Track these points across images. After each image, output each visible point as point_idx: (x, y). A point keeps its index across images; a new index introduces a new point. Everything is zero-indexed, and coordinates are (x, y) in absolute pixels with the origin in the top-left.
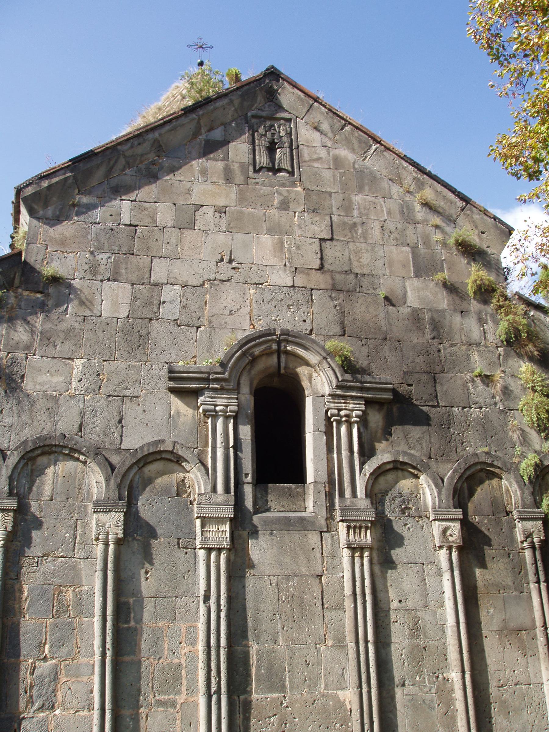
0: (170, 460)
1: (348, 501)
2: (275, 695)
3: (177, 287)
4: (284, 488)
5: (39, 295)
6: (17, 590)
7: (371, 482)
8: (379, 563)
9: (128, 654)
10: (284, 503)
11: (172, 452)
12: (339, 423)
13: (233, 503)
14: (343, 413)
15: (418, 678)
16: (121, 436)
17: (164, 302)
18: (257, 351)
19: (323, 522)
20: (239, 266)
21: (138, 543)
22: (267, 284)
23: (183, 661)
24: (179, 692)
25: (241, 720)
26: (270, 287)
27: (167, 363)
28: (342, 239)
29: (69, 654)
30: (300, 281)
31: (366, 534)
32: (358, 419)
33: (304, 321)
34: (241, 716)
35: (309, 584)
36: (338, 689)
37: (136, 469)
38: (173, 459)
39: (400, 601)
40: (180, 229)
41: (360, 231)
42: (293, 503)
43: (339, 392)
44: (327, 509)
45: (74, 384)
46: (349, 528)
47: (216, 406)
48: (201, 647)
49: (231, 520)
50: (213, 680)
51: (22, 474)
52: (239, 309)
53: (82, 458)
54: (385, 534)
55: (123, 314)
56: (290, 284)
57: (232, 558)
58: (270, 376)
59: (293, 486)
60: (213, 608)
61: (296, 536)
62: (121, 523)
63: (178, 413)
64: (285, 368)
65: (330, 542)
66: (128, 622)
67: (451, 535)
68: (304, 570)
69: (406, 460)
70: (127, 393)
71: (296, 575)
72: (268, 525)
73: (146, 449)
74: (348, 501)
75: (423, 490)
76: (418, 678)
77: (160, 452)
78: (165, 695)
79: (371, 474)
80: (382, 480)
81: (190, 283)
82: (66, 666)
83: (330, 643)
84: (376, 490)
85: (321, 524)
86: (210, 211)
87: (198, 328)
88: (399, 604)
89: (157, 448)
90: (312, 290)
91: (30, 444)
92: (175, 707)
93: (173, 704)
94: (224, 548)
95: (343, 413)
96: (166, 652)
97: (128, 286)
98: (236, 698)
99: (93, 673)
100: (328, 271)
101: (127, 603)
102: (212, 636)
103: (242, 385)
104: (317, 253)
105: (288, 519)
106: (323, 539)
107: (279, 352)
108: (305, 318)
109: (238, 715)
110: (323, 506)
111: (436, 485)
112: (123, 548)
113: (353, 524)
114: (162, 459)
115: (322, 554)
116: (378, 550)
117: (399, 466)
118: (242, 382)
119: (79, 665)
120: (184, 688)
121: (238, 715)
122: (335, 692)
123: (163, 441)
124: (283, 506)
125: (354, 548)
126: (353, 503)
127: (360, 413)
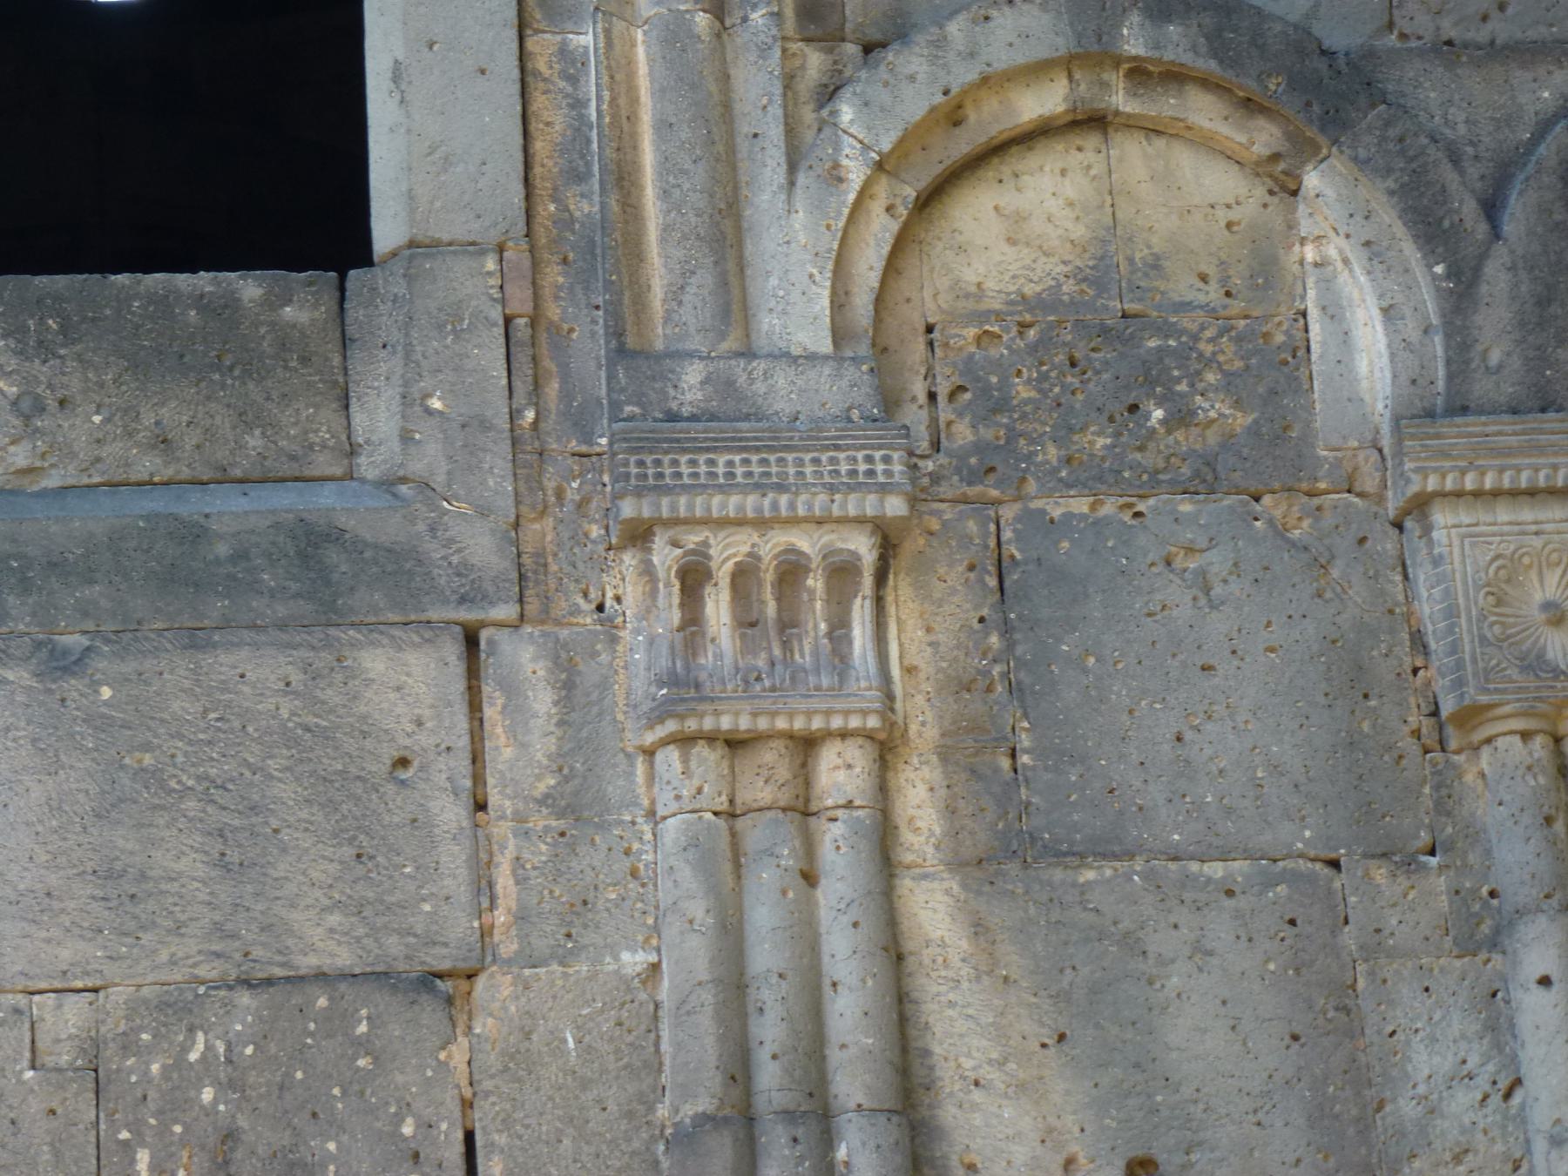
1: (692, 375)
4: (163, 304)
7: (880, 230)
8: (957, 864)
10: (172, 414)
19: (481, 547)
35: (363, 1045)
42: (247, 419)
44: (515, 442)
46: (693, 578)
54: (1007, 629)
59: (249, 287)
61: (259, 673)
65: (543, 701)
68: (324, 942)
71: (246, 983)
72: (25, 586)
74: (692, 375)
75: (1327, 284)
80: (977, 212)
85: (462, 571)
105: (194, 534)
106: (487, 689)
110: (485, 426)
111: (1431, 227)
113: (727, 551)
115: (481, 806)
116: (945, 755)
117: (1120, 100)
124: (163, 443)
125: (735, 744)
126: (724, 386)
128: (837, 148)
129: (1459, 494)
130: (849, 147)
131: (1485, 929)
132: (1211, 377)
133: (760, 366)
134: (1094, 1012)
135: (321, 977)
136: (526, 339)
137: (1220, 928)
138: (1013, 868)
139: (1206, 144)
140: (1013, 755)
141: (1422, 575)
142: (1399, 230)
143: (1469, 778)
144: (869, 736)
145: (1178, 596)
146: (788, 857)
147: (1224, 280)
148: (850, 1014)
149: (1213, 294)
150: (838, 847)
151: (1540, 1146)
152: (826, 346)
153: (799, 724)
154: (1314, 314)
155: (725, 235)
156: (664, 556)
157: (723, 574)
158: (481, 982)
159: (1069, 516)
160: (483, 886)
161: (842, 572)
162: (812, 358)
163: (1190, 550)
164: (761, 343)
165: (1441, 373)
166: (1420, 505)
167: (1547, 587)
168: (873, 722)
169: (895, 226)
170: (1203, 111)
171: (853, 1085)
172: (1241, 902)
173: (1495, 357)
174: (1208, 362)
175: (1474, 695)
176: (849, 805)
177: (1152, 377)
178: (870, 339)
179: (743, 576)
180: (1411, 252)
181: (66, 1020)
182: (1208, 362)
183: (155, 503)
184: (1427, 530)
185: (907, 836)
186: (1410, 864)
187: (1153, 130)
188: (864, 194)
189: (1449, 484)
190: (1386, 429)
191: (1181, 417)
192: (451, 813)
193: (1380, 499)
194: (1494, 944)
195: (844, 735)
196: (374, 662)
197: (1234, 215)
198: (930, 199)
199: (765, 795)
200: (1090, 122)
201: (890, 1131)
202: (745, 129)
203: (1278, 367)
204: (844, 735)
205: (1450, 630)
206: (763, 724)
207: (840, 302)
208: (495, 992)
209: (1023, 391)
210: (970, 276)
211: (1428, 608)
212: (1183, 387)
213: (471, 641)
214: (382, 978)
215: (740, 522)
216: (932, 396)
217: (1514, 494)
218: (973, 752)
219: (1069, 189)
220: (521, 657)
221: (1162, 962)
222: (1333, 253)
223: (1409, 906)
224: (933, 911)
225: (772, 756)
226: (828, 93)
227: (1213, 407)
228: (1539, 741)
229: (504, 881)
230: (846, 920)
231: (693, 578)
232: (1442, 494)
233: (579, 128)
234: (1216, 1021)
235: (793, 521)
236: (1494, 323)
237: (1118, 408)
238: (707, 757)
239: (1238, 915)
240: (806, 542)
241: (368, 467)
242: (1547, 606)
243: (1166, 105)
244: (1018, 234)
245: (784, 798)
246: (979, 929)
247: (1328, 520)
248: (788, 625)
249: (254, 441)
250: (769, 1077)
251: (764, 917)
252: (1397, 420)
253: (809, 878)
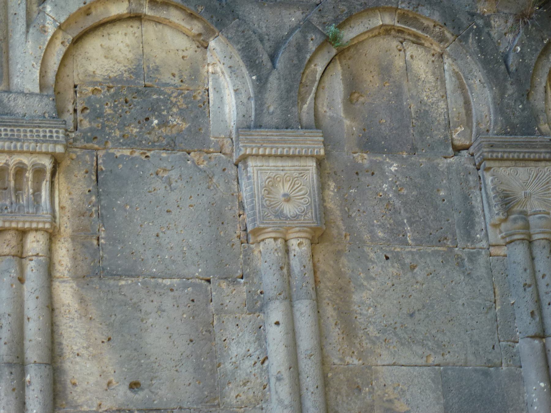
7: (58, 50)
8: (75, 277)
31: (37, 191)
39: (134, 386)
54: (98, 195)
67: (288, 198)
75: (216, 80)
80: (94, 46)
84: (77, 72)
88: (129, 394)
111: (252, 64)
116: (73, 238)
128: (45, 20)
129: (257, 155)
130: (49, 20)
131: (258, 305)
132: (175, 110)
133: (12, 96)
134: (122, 331)
137: (168, 303)
138: (96, 279)
139: (176, 28)
140: (98, 239)
141: (244, 182)
142: (241, 63)
143: (256, 253)
144: (46, 231)
145: (159, 186)
146: (14, 272)
147: (181, 76)
148: (34, 330)
149: (177, 81)
150: (33, 270)
151: (273, 380)
152: (37, 90)
153: (20, 225)
154: (211, 90)
159: (123, 156)
161: (39, 172)
162: (32, 94)
163: (165, 170)
164: (13, 88)
165: (253, 113)
166: (244, 158)
167: (285, 189)
168: (47, 226)
169: (64, 49)
171: (33, 354)
172: (176, 293)
173: (272, 109)
174: (174, 105)
175: (258, 224)
176: (37, 255)
177: (154, 109)
178: (54, 88)
180: (245, 71)
182: (174, 105)
184: (246, 167)
185: (58, 267)
186: (234, 282)
187: (158, 22)
188: (53, 37)
189: (254, 152)
190: (234, 132)
191: (164, 123)
193: (231, 156)
194: (261, 310)
195: (37, 230)
197: (185, 54)
198: (77, 41)
200: (136, 17)
201: (45, 371)
202: (12, 11)
203: (198, 108)
204: (37, 230)
205: (252, 202)
206: (7, 225)
207: (43, 75)
209: (108, 111)
210: (91, 69)
211: (245, 194)
212: (165, 113)
216: (75, 111)
217: (276, 156)
218: (84, 238)
219: (127, 40)
221: (147, 313)
222: (218, 69)
223: (232, 296)
224: (66, 294)
227: (175, 120)
228: (280, 241)
230: (34, 296)
232: (251, 155)
234: (164, 335)
235: (22, 152)
237: (141, 119)
239: (174, 298)
240: (26, 160)
242: (285, 195)
243: (162, 14)
244: (108, 55)
245: (13, 252)
246: (82, 300)
247: (213, 162)
248: (18, 189)
252: (237, 129)
253: (21, 280)
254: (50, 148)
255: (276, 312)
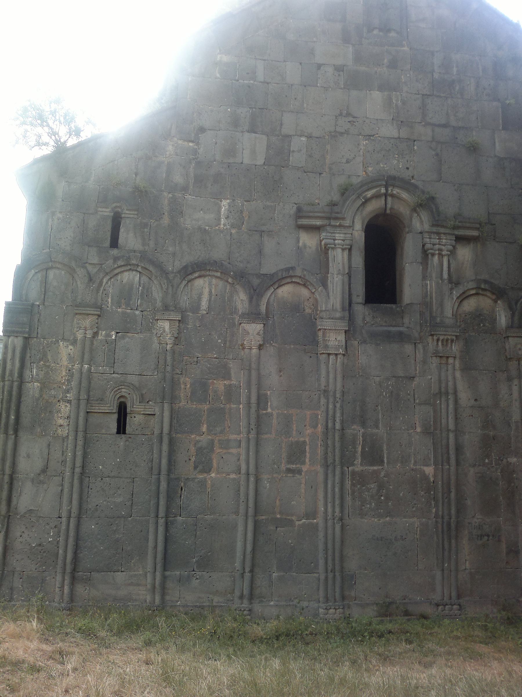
0: (298, 283)
2: (375, 468)
3: (303, 139)
5: (191, 144)
6: (182, 382)
7: (457, 304)
9: (266, 434)
11: (300, 277)
12: (433, 255)
13: (348, 319)
14: (437, 247)
15: (487, 461)
16: (260, 263)
17: (293, 151)
18: (369, 194)
19: (417, 335)
20: (354, 120)
21: (274, 349)
22: (377, 135)
23: (307, 440)
24: (304, 463)
25: (349, 485)
26: (380, 138)
27: (296, 204)
28: (442, 95)
29: (222, 432)
30: (404, 133)
31: (452, 345)
32: (449, 253)
33: (408, 168)
34: (350, 483)
36: (425, 466)
37: (272, 290)
38: (301, 282)
39: (476, 400)
40: (305, 86)
41: (457, 88)
43: (434, 229)
45: (223, 221)
46: (438, 340)
47: (334, 240)
48: (320, 428)
49: (346, 332)
50: (330, 454)
51: (183, 293)
52: (354, 158)
53: (230, 280)
55: (260, 161)
56: (396, 135)
57: (346, 361)
58: (377, 216)
59: (394, 306)
60: (331, 400)
62: (262, 332)
63: (305, 246)
64: (391, 209)
65: (422, 351)
66: (266, 409)
67: (520, 349)
68: (401, 374)
69: (487, 287)
70: (264, 228)
71: (394, 377)
73: (280, 274)
74: (438, 319)
76: (487, 461)
77: (291, 277)
78: (293, 464)
79: (458, 298)
81: (314, 135)
82: (219, 440)
83: (419, 430)
86: (330, 70)
87: (320, 174)
89: (288, 273)
90: (414, 141)
91: (190, 269)
92: (301, 474)
93: (299, 472)
94: (340, 354)
95: (437, 247)
96: (294, 433)
97: (264, 137)
98: (346, 469)
99: (239, 446)
100: (428, 124)
101: (266, 395)
102: (329, 421)
103: (355, 222)
104: (420, 108)
105: (389, 332)
107: (386, 195)
108: (408, 166)
109: (347, 482)
111: (511, 308)
112: (262, 352)
113: (441, 338)
114: (292, 282)
117: (481, 292)
118: (355, 221)
119: (228, 441)
120: (307, 460)
121: (347, 482)
122: (422, 467)
123: (293, 268)
124: (386, 322)
125: (441, 357)
127: (450, 248)
130: (454, 296)
135: (401, 377)
136: (422, 314)
139: (489, 297)
148: (450, 384)
149: (488, 313)
150: (450, 367)
151: (514, 401)
155: (441, 305)
156: (435, 338)
157: (441, 340)
158: (415, 379)
160: (416, 370)
161: (452, 341)
166: (508, 337)
170: (489, 294)
171: (451, 391)
178: (455, 315)
179: (443, 340)
181: (378, 379)
183: (386, 328)
187: (483, 295)
190: (504, 329)
191: (484, 326)
192: (413, 362)
196: (406, 346)
199: (444, 362)
200: (477, 294)
203: (494, 321)
208: (417, 379)
211: (507, 347)
213: (415, 343)
214: (406, 377)
215: (443, 335)
220: (420, 346)
225: (445, 359)
226: (451, 289)
229: (418, 368)
231: (438, 340)
233: (427, 292)
236: (516, 318)
238: (438, 359)
240: (449, 337)
241: (405, 325)
243: (485, 293)
244: (470, 305)
248: (447, 345)
249: (394, 322)
250: (443, 390)
251: (443, 374)
254: (456, 334)
255: (516, 382)
